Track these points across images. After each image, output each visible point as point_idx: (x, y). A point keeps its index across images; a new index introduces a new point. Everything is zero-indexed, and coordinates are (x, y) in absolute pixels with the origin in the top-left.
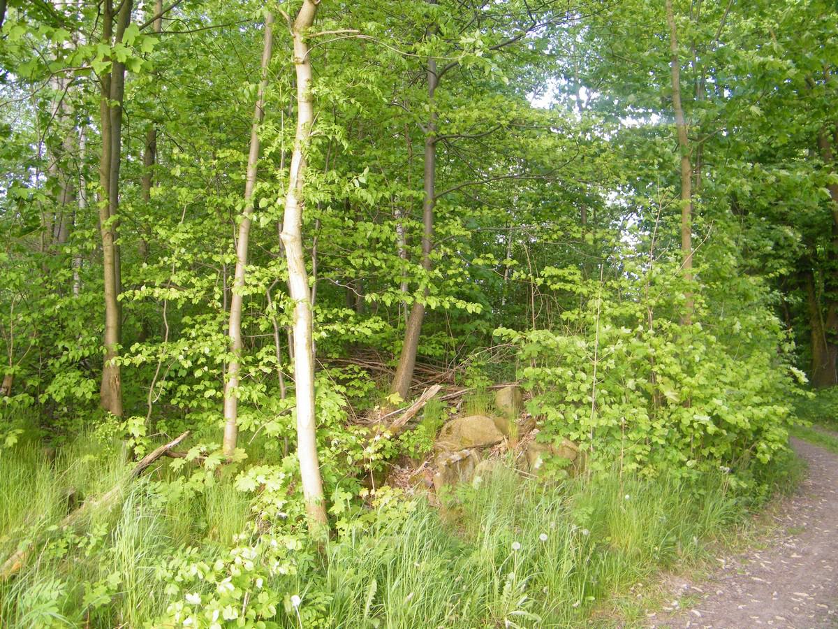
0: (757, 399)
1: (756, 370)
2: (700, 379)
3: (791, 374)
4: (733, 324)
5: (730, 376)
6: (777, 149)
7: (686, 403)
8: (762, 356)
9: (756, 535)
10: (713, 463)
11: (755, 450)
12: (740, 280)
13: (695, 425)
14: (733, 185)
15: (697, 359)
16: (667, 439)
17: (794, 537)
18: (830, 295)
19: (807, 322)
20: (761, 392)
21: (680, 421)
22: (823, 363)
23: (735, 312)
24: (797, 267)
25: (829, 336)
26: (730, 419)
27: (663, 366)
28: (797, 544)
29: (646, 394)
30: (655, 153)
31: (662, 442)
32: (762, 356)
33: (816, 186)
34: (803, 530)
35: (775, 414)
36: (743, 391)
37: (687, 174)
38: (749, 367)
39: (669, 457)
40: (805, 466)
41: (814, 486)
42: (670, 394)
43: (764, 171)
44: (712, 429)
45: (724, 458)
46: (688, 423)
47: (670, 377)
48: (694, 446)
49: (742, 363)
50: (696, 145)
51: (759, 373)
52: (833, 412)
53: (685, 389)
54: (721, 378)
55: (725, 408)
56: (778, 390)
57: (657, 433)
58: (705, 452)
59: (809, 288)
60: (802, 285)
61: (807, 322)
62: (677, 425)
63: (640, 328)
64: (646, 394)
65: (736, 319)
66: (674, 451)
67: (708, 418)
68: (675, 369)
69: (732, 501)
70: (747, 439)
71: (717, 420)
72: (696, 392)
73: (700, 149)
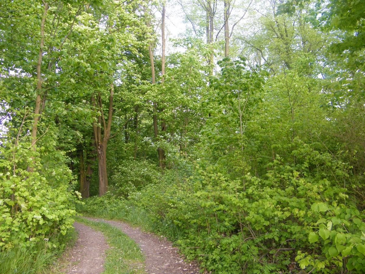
0: (62, 206)
1: (61, 193)
2: (38, 197)
3: (76, 194)
4: (52, 172)
5: (50, 195)
6: (75, 98)
7: (30, 210)
8: (64, 186)
9: (60, 268)
10: (41, 237)
11: (60, 229)
12: (56, 152)
13: (34, 220)
14: (59, 111)
15: (36, 188)
16: (19, 228)
17: (76, 266)
18: (89, 160)
19: (79, 171)
20: (63, 203)
21: (27, 219)
22: (84, 188)
23: (54, 166)
24: (77, 148)
25: (87, 177)
26: (50, 217)
27: (20, 193)
28: (77, 269)
29: (10, 207)
30: (25, 90)
31: (17, 230)
32: (64, 186)
33: (92, 116)
34: (79, 262)
35: (69, 213)
36: (56, 202)
37: (38, 102)
38: (58, 192)
39: (20, 237)
40: (78, 233)
41: (82, 242)
42: (23, 206)
43: (73, 107)
44: (41, 222)
45: (46, 235)
46: (31, 220)
47: (23, 197)
48: (32, 230)
49: (56, 190)
50: (44, 90)
51: (63, 194)
52: (87, 209)
53: (30, 203)
54: (47, 197)
55: (47, 212)
56: (70, 201)
57: (14, 226)
58: (37, 233)
59: (81, 157)
60: (78, 156)
61: (79, 171)
62: (25, 221)
63: (8, 174)
64: (10, 207)
65: (54, 170)
66: (23, 234)
67: (40, 217)
68: (26, 194)
69: (49, 255)
70: (56, 225)
71: (44, 217)
72: (35, 204)
73: (46, 93)
